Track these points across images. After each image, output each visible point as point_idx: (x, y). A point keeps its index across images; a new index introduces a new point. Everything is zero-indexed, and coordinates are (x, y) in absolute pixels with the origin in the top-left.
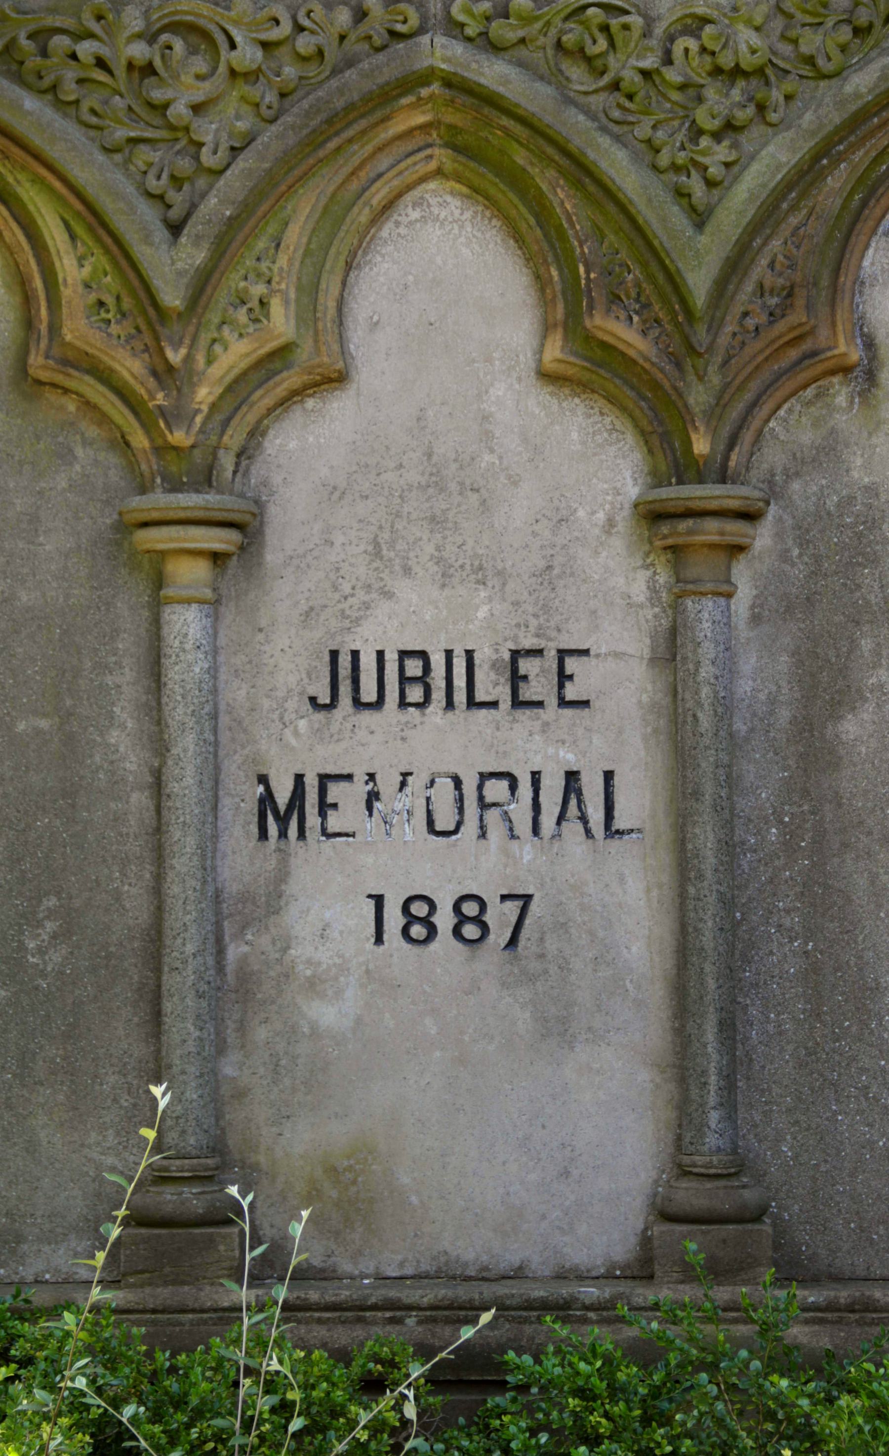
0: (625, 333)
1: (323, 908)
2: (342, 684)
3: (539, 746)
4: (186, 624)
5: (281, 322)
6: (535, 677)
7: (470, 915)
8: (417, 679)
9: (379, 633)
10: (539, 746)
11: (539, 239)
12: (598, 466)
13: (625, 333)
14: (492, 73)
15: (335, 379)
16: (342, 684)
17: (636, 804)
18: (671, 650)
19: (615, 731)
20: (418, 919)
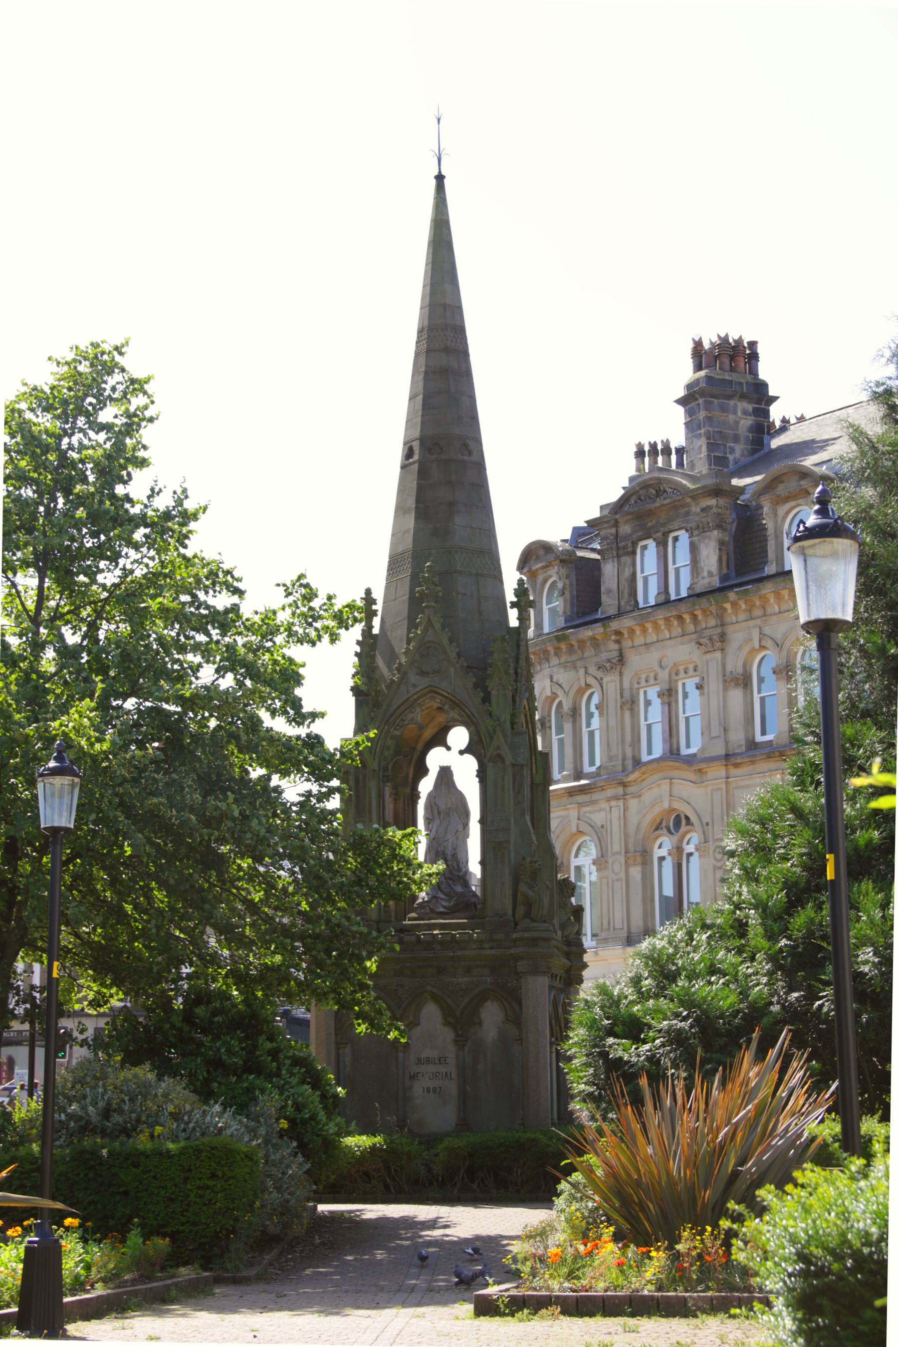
0: (451, 1020)
1: (418, 1089)
2: (419, 1061)
3: (442, 1069)
4: (401, 1055)
5: (411, 1019)
6: (442, 1060)
7: (434, 1090)
8: (428, 1061)
9: (424, 1055)
10: (442, 1069)
11: (442, 1008)
12: (447, 1035)
13: (451, 1020)
14: (435, 990)
15: (419, 1024)
16: (419, 1061)
17: (454, 1076)
18: (457, 1057)
19: (451, 1067)
20: (428, 1090)
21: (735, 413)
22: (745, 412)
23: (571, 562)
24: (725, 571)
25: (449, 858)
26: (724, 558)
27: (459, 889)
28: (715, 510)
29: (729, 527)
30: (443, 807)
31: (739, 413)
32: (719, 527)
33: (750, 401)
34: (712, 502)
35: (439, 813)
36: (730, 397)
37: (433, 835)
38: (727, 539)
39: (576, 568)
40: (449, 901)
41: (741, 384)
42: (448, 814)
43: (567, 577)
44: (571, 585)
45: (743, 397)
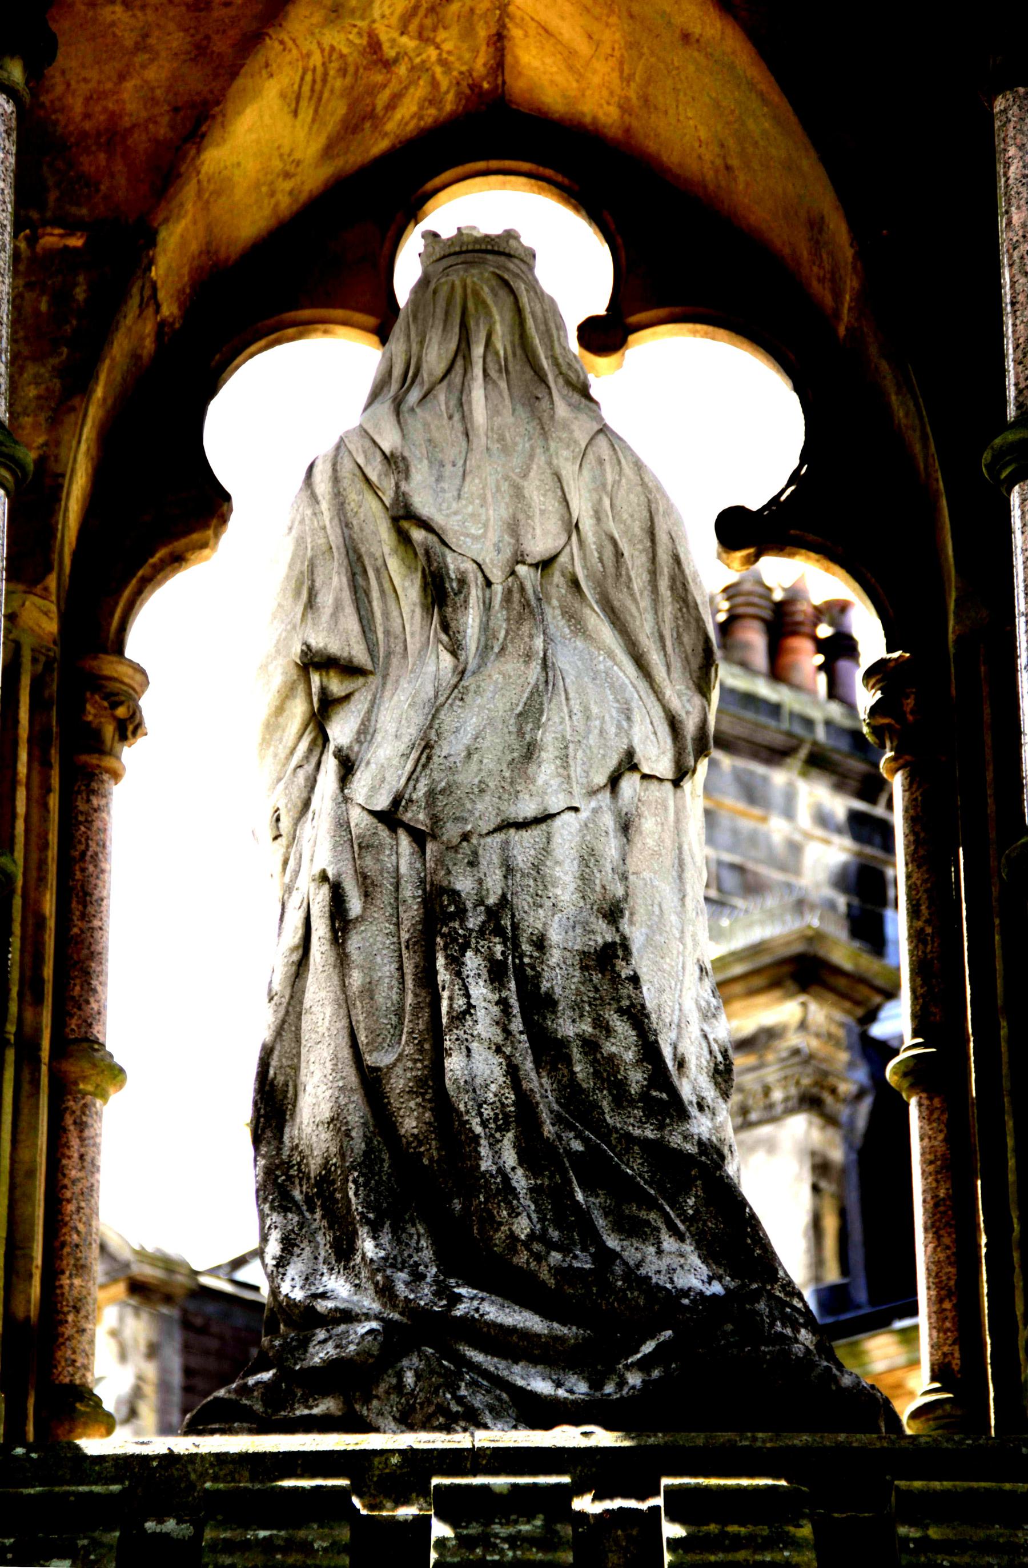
21: (789, 813)
22: (822, 819)
23: (168, 1299)
24: (832, 1275)
25: (559, 976)
26: (831, 1224)
27: (686, 1269)
28: (794, 1040)
29: (844, 1112)
30: (475, 532)
31: (804, 818)
32: (810, 1102)
33: (840, 786)
34: (782, 1011)
35: (439, 592)
36: (775, 755)
37: (372, 789)
38: (837, 1155)
39: (186, 1324)
40: (592, 1359)
41: (808, 723)
42: (525, 608)
43: (153, 1351)
44: (163, 1386)
45: (818, 762)
